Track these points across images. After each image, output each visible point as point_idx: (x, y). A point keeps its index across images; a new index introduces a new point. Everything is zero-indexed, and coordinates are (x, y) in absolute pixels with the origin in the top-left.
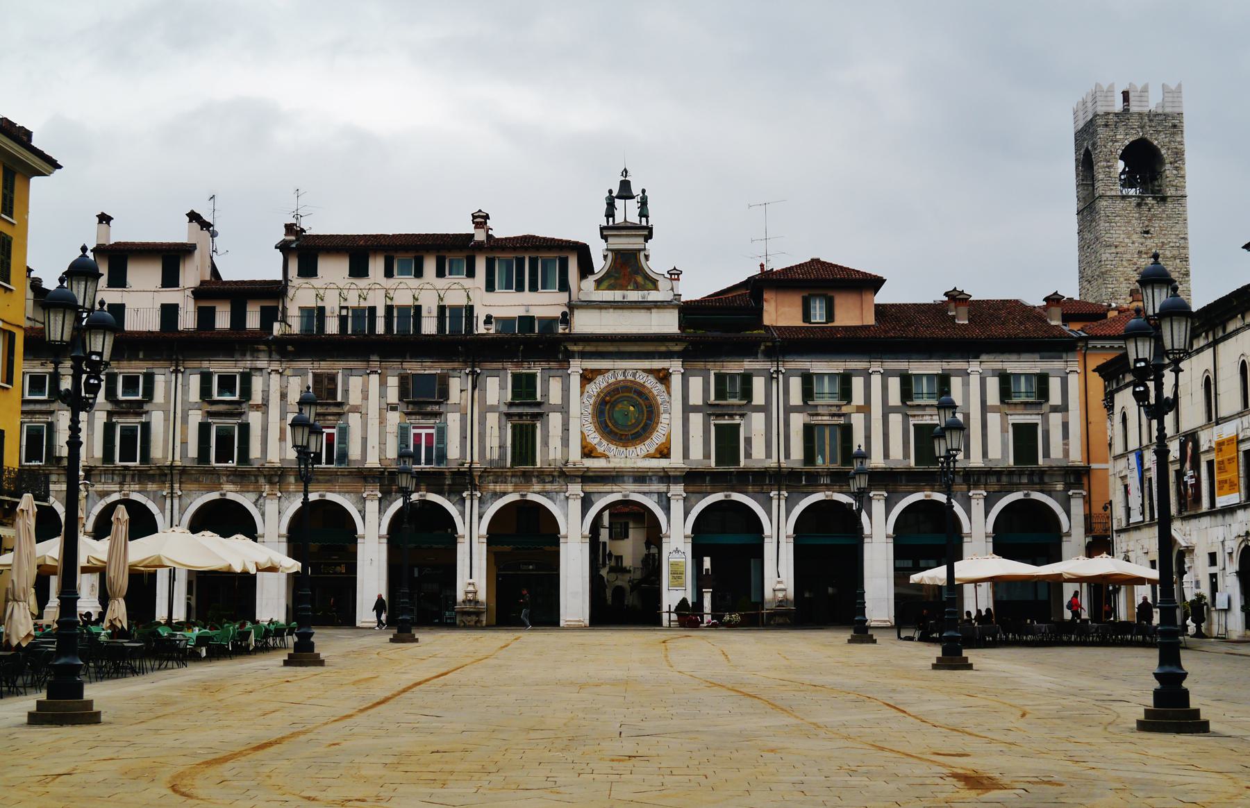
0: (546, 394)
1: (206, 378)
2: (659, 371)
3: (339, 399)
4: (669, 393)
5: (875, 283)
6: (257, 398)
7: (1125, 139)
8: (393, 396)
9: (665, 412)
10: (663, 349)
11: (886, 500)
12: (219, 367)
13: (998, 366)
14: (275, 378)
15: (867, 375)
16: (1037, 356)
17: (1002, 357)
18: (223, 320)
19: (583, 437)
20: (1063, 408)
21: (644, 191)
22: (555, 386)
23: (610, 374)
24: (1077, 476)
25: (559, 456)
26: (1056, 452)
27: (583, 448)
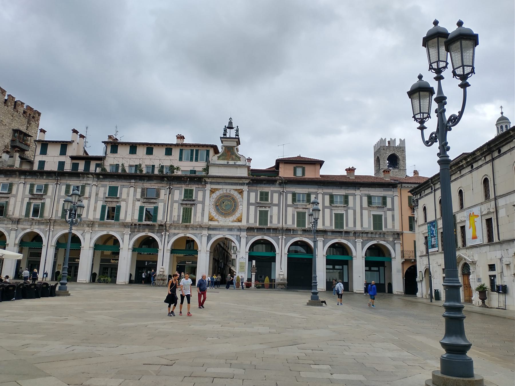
0: (196, 197)
1: (68, 187)
2: (239, 190)
3: (118, 196)
4: (242, 198)
5: (321, 163)
6: (87, 195)
7: (389, 154)
8: (139, 196)
9: (241, 205)
10: (241, 182)
11: (323, 241)
12: (74, 182)
13: (367, 193)
14: (94, 188)
15: (317, 194)
16: (382, 189)
17: (370, 189)
18: (81, 168)
19: (210, 213)
20: (392, 209)
21: (237, 127)
22: (200, 194)
23: (221, 190)
24: (398, 235)
25: (200, 220)
26: (390, 226)
27: (209, 217)
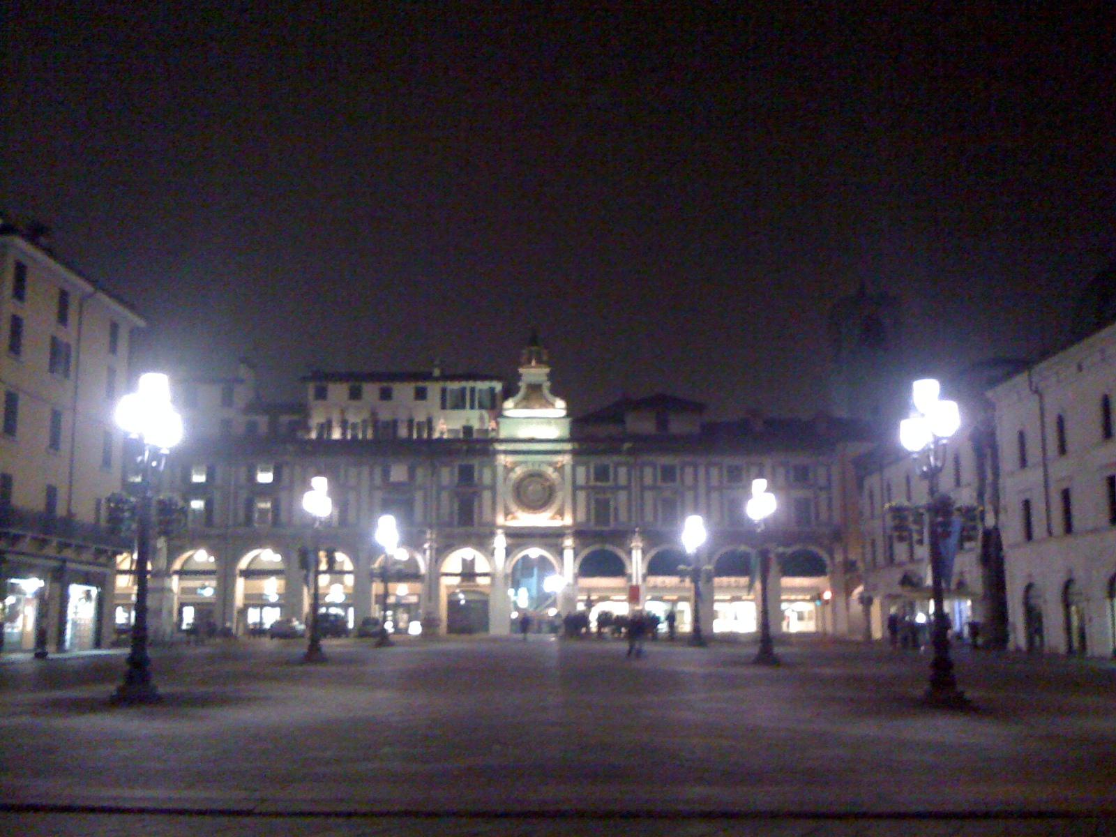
0: (480, 478)
15: (696, 467)
20: (828, 487)
